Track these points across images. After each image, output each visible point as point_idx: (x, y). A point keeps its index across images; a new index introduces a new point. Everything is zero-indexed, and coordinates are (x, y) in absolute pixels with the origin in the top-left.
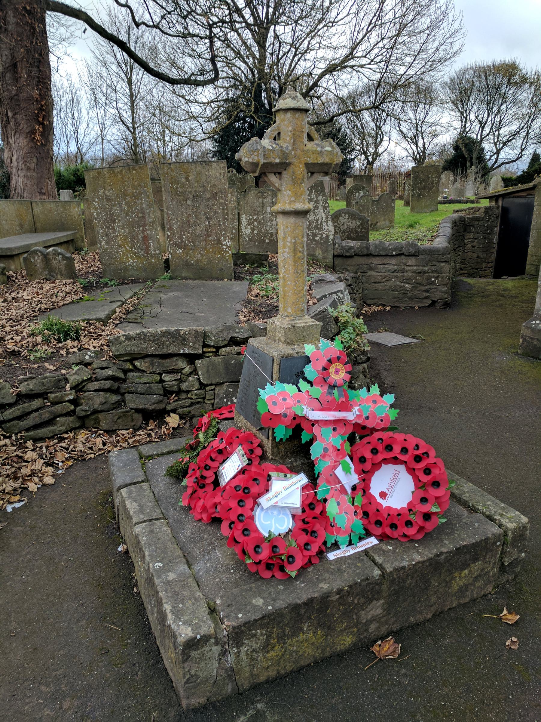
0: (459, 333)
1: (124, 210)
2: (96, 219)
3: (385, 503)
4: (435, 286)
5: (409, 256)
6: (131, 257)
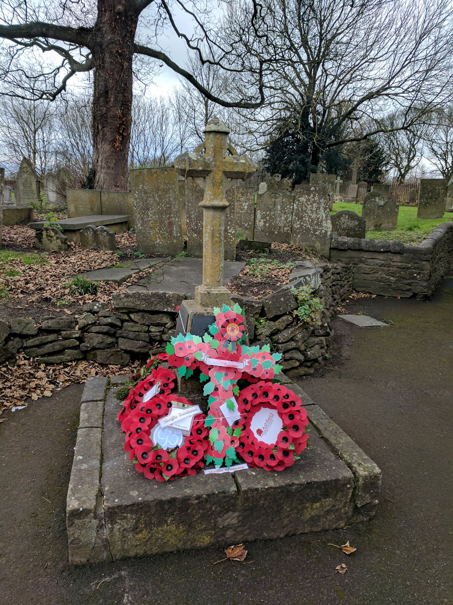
0: (426, 322)
1: (156, 201)
2: (135, 207)
3: (260, 439)
4: (417, 281)
5: (394, 253)
6: (159, 237)
